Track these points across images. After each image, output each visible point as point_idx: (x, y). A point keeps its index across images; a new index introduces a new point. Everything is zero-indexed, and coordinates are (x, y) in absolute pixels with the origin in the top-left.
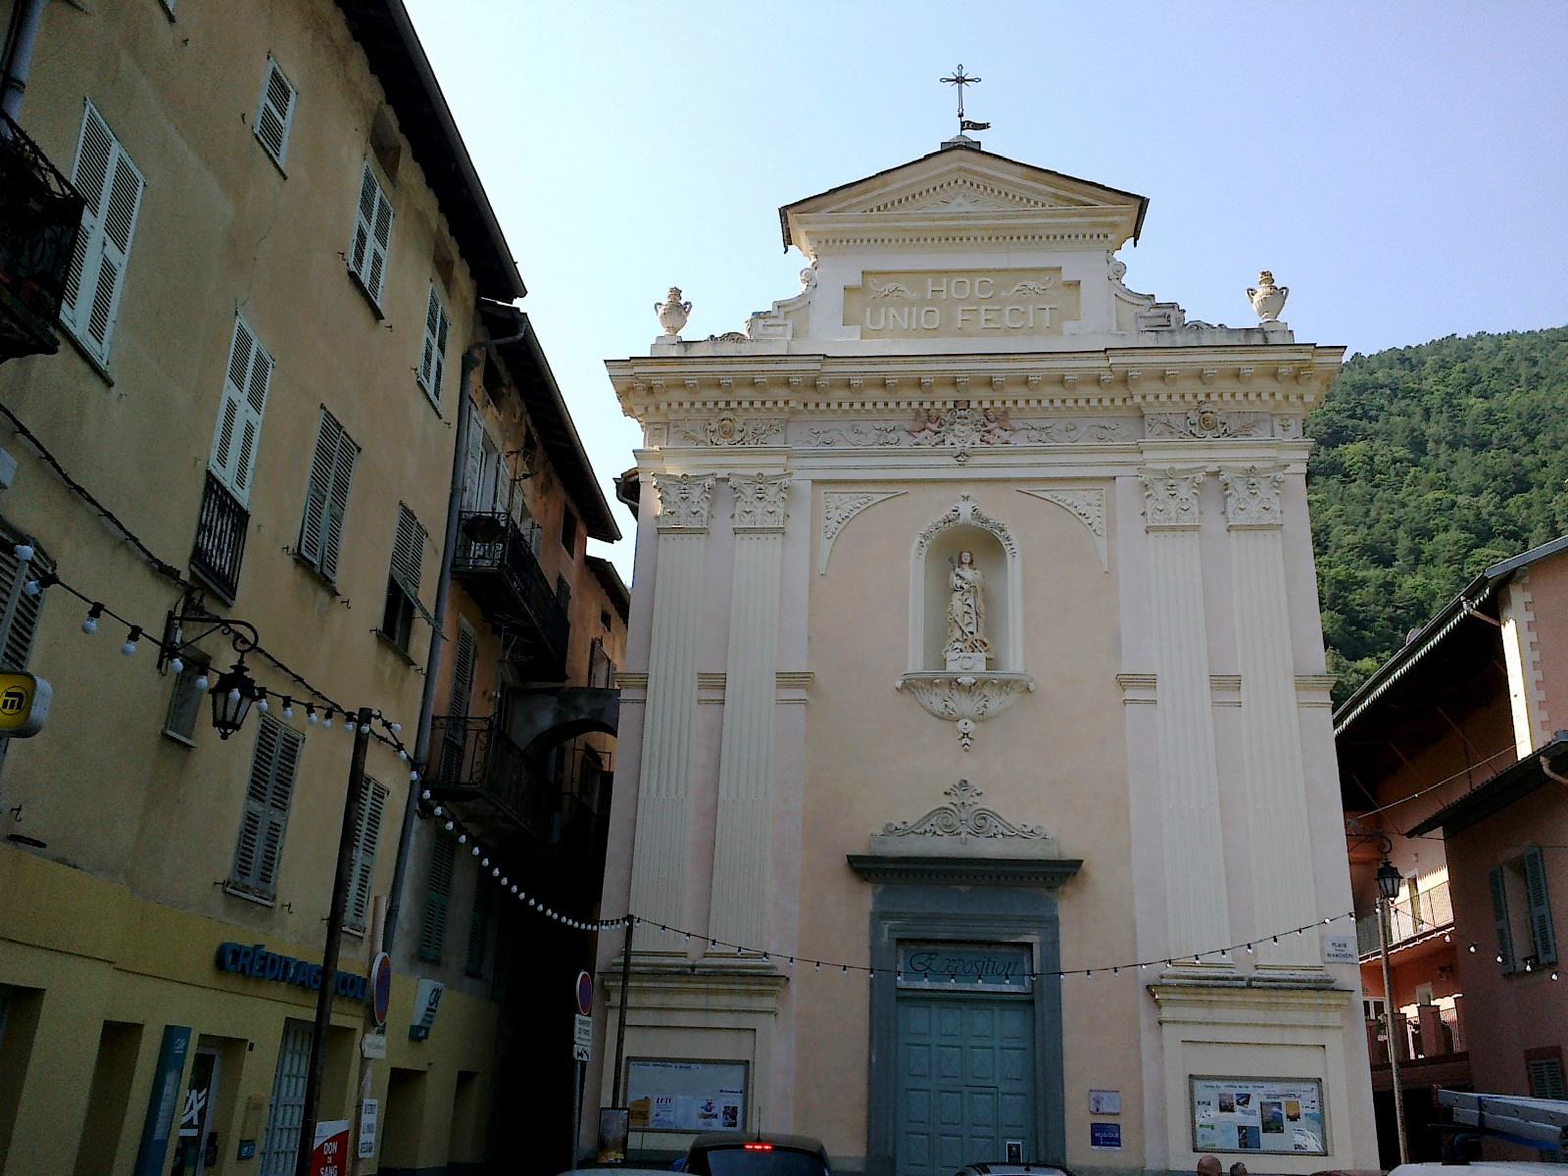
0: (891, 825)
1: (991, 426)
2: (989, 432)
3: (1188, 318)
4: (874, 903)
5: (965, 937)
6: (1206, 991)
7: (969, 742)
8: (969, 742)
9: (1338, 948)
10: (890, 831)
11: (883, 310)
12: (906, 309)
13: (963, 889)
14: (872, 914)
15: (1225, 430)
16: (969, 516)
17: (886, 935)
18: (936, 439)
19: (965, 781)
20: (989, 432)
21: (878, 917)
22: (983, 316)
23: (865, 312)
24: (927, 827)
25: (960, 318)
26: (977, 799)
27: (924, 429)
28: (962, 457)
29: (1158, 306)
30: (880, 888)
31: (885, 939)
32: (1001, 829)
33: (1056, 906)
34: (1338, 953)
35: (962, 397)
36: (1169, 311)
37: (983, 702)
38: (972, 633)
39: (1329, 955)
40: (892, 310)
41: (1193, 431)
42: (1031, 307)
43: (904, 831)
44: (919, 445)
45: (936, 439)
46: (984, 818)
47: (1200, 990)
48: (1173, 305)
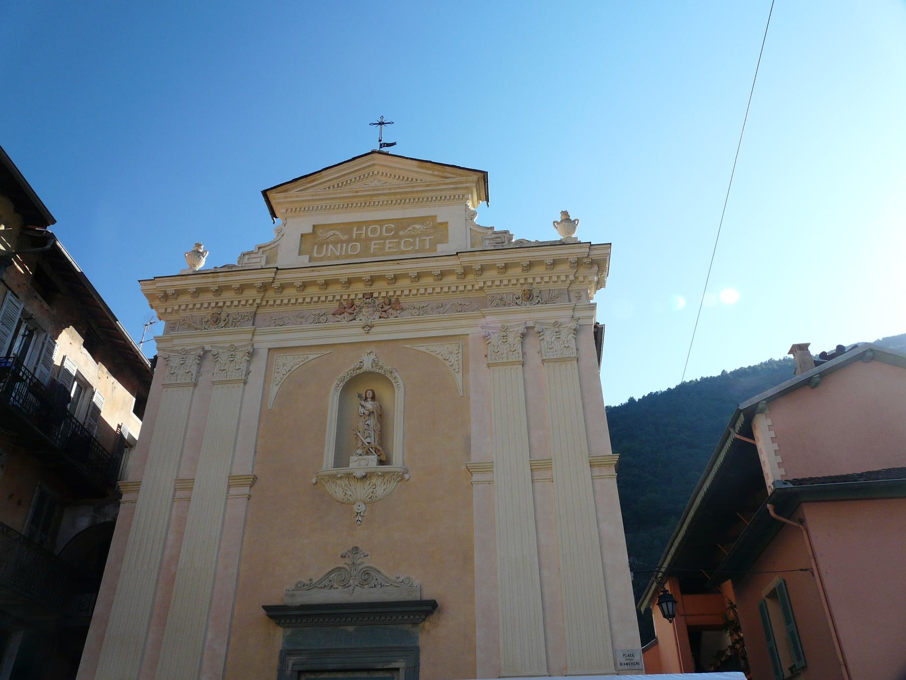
1: (386, 308)
2: (385, 311)
8: (360, 519)
10: (300, 586)
11: (325, 246)
12: (339, 245)
13: (351, 629)
14: (281, 651)
16: (370, 367)
17: (290, 668)
18: (351, 317)
19: (357, 548)
20: (385, 311)
21: (285, 654)
22: (387, 246)
23: (314, 248)
24: (326, 582)
25: (373, 247)
27: (344, 313)
28: (368, 327)
30: (289, 631)
31: (289, 672)
32: (380, 581)
35: (368, 290)
37: (371, 490)
40: (331, 246)
42: (417, 239)
43: (311, 586)
44: (339, 322)
45: (351, 317)
46: (367, 573)
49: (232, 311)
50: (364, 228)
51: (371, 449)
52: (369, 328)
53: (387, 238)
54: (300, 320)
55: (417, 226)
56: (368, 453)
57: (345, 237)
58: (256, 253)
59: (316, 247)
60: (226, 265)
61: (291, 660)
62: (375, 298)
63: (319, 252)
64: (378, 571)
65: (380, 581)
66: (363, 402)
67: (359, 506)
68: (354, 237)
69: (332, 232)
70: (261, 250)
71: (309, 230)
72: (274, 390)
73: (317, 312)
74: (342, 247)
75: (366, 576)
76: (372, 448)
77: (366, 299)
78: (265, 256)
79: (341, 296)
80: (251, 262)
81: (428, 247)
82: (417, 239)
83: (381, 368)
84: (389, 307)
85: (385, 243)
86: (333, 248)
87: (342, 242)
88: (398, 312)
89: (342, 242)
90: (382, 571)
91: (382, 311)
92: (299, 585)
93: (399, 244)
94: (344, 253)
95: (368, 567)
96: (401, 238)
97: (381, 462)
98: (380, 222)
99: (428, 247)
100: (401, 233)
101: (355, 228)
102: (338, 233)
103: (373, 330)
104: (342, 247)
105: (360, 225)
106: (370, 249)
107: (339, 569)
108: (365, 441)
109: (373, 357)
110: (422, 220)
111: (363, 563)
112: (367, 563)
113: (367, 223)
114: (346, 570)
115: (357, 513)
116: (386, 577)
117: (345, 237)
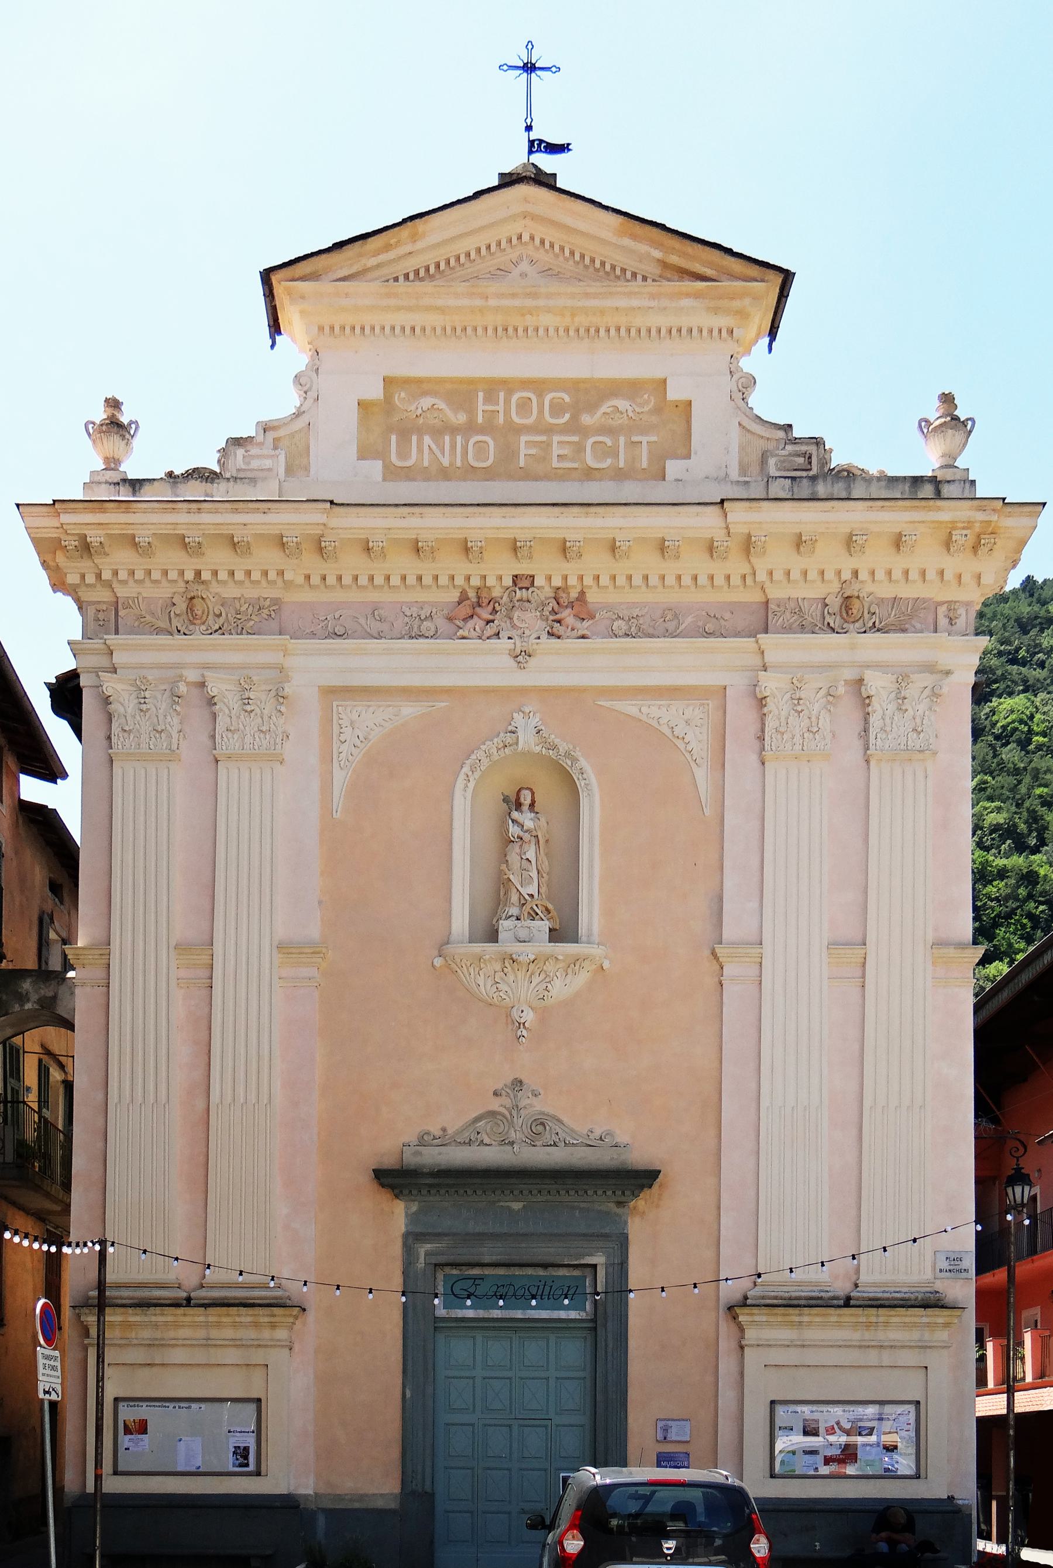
0: (428, 1133)
3: (837, 461)
4: (406, 1225)
5: (516, 1258)
6: (796, 1311)
7: (525, 1033)
8: (525, 1033)
9: (952, 1263)
13: (516, 1206)
14: (406, 1236)
15: (874, 623)
17: (422, 1260)
19: (521, 1082)
20: (559, 621)
21: (412, 1239)
22: (556, 451)
25: (523, 451)
26: (534, 1101)
28: (521, 657)
29: (796, 441)
30: (414, 1207)
31: (421, 1263)
33: (626, 1223)
34: (951, 1268)
35: (523, 568)
36: (812, 449)
38: (532, 896)
39: (941, 1271)
40: (427, 440)
41: (832, 625)
42: (622, 440)
43: (443, 1140)
46: (543, 1124)
47: (791, 1310)
48: (818, 442)
49: (230, 592)
50: (502, 395)
51: (535, 908)
52: (528, 658)
53: (550, 430)
54: (375, 626)
55: (622, 404)
56: (533, 916)
57: (461, 418)
58: (262, 444)
59: (394, 438)
60: (195, 470)
61: (423, 1249)
62: (538, 588)
63: (403, 454)
64: (559, 1120)
65: (562, 1135)
66: (515, 815)
67: (522, 1011)
68: (480, 420)
69: (426, 402)
70: (271, 435)
71: (375, 391)
72: (340, 778)
73: (414, 611)
74: (453, 447)
75: (540, 1128)
76: (536, 905)
77: (521, 589)
78: (282, 458)
79: (468, 578)
80: (251, 467)
81: (645, 465)
82: (622, 440)
83: (555, 747)
84: (569, 610)
85: (549, 445)
86: (433, 447)
87: (454, 430)
88: (586, 624)
89: (454, 430)
90: (565, 1120)
91: (553, 621)
92: (425, 1137)
93: (580, 448)
94: (459, 464)
95: (543, 1113)
96: (585, 432)
97: (555, 935)
98: (539, 386)
99: (645, 465)
100: (586, 419)
101: (481, 395)
102: (442, 405)
103: (533, 662)
104: (453, 447)
105: (494, 387)
106: (515, 454)
107: (492, 1114)
108: (525, 892)
109: (535, 721)
110: (632, 388)
111: (531, 1105)
112: (538, 1106)
113: (508, 385)
114: (504, 1116)
115: (520, 1024)
116: (572, 1130)
117: (461, 418)
